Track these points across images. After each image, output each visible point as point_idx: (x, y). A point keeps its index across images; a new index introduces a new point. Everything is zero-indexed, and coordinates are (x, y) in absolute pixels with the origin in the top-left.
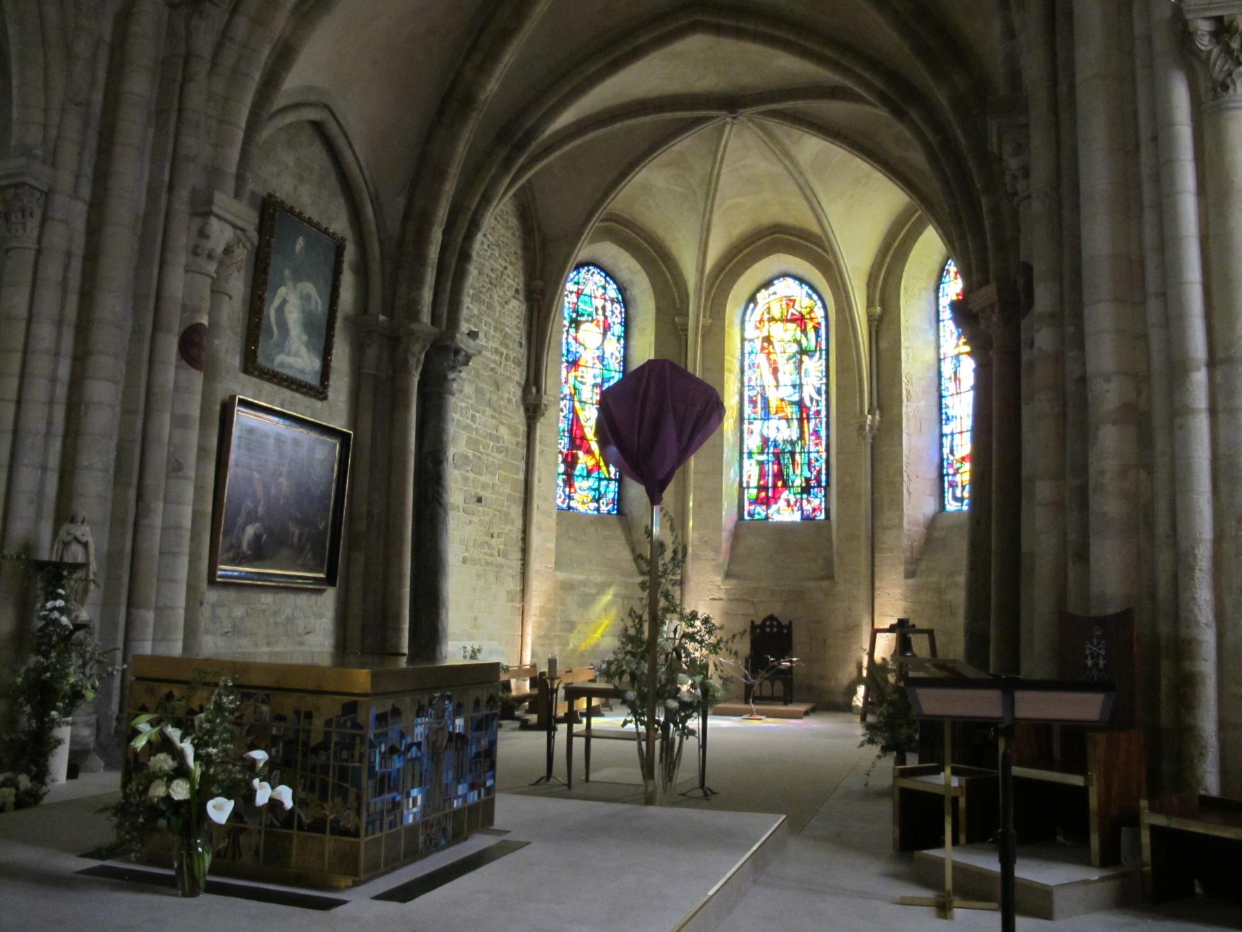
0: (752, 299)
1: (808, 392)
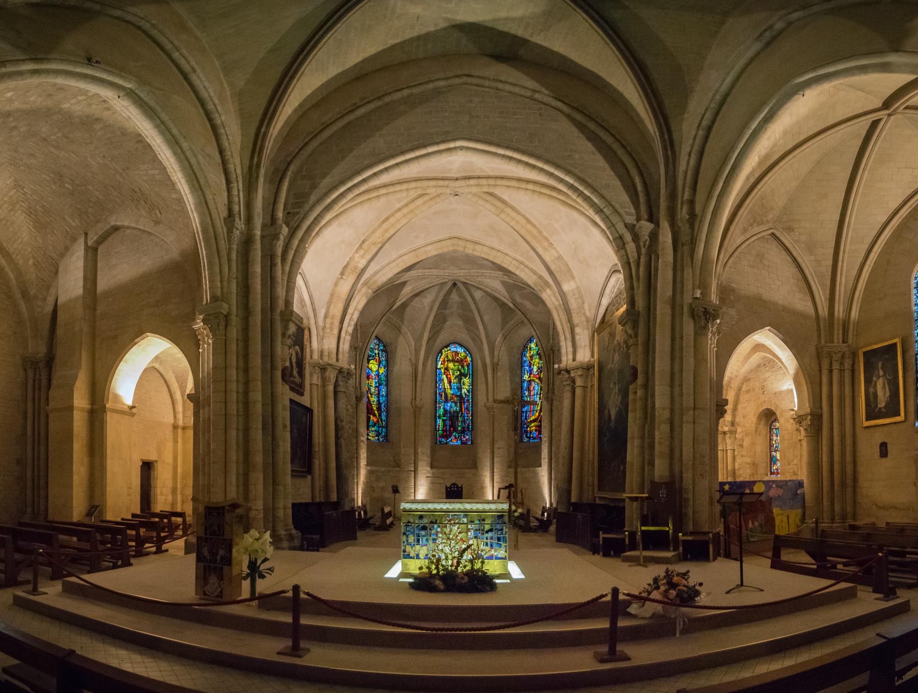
0: (441, 352)
1: (464, 391)
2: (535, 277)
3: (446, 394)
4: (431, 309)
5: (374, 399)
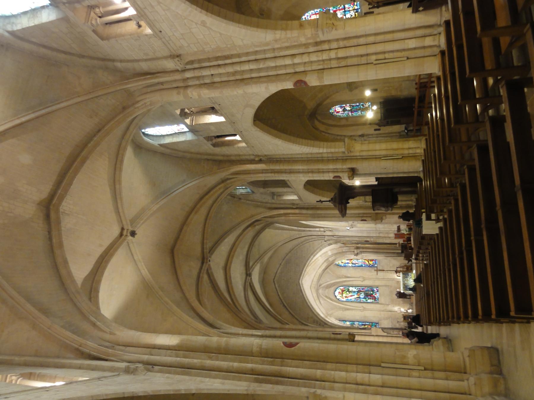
1: (355, 290)
4: (326, 300)
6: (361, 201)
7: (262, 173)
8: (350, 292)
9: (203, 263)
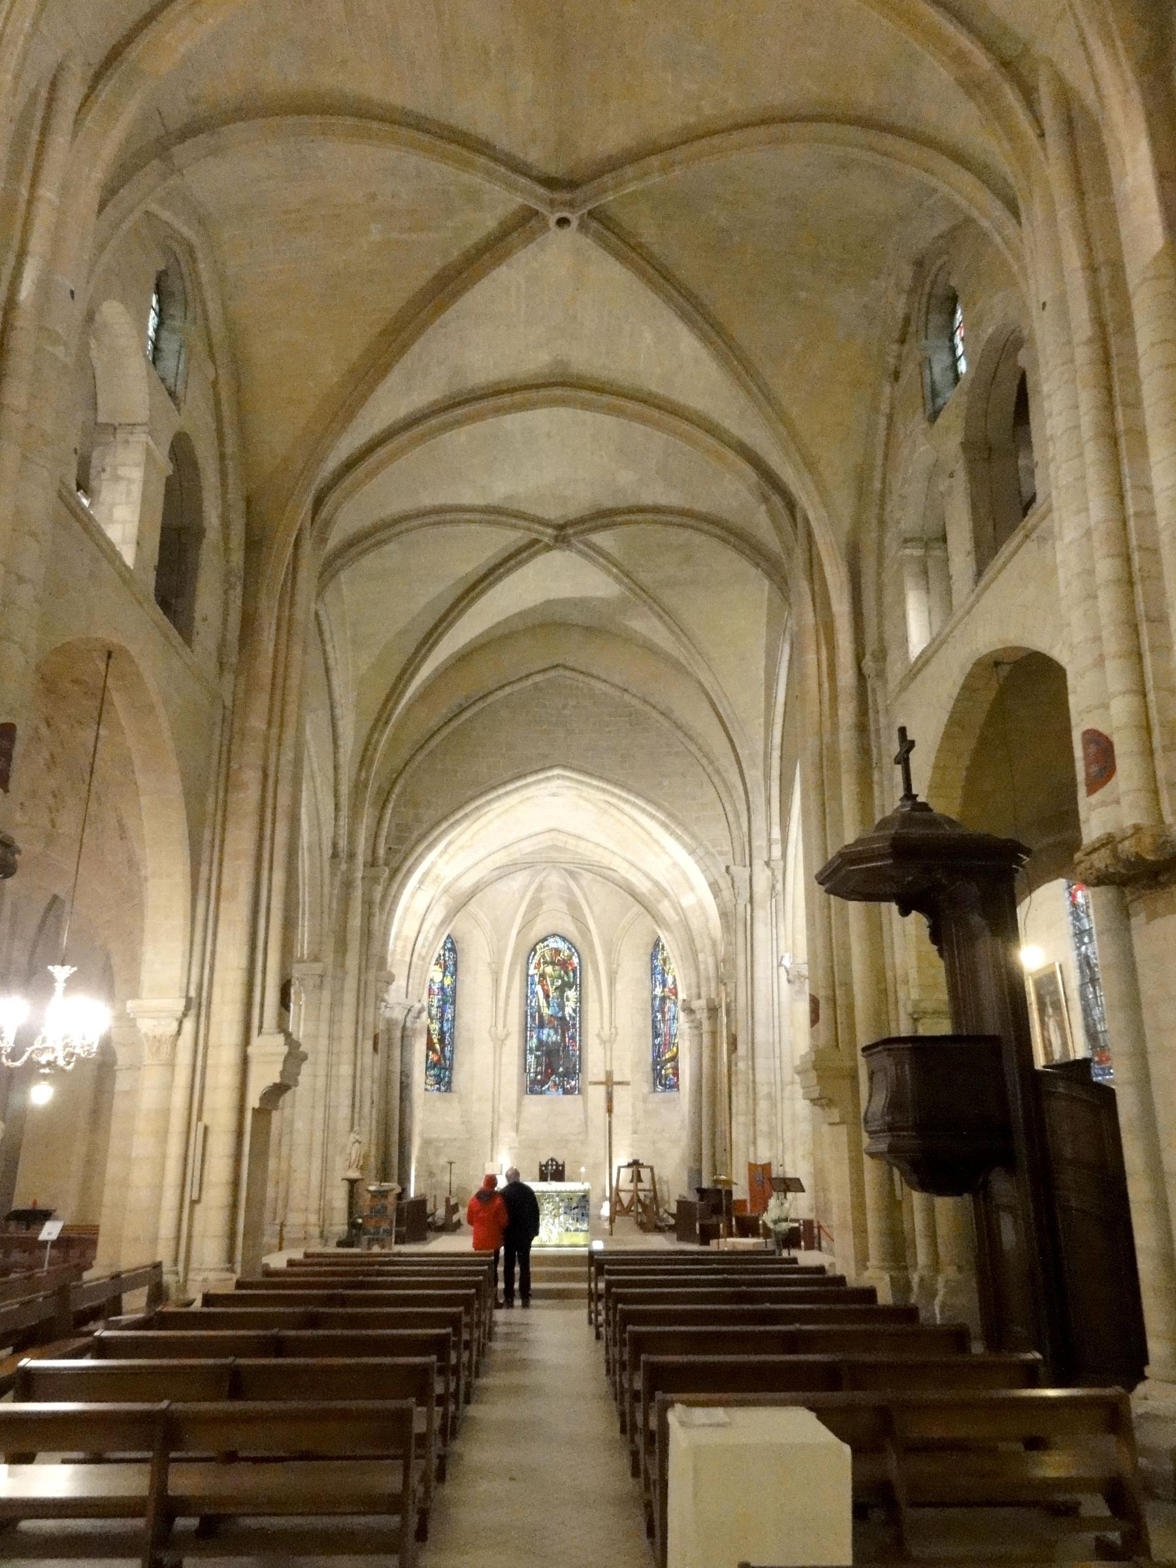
0: (534, 949)
1: (568, 1010)
2: (649, 885)
3: (541, 1016)
4: (522, 898)
5: (435, 1026)
6: (915, 994)
7: (1092, 269)
8: (561, 990)
9: (550, 182)
